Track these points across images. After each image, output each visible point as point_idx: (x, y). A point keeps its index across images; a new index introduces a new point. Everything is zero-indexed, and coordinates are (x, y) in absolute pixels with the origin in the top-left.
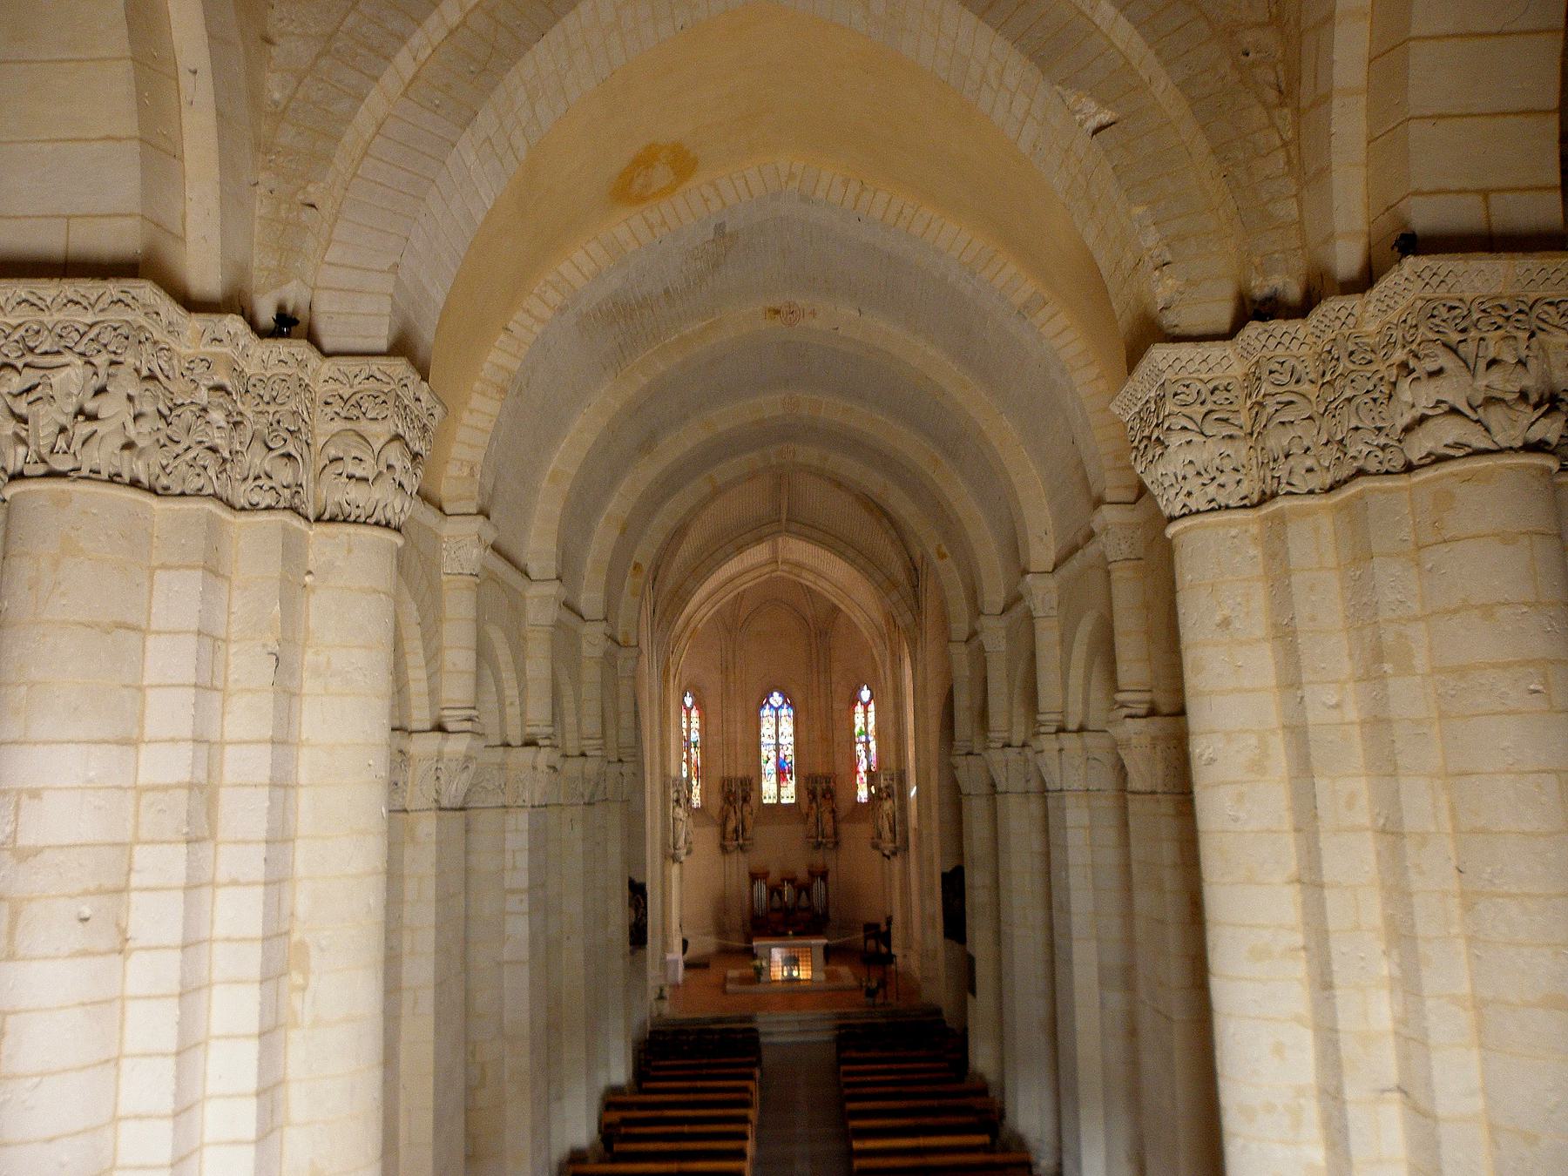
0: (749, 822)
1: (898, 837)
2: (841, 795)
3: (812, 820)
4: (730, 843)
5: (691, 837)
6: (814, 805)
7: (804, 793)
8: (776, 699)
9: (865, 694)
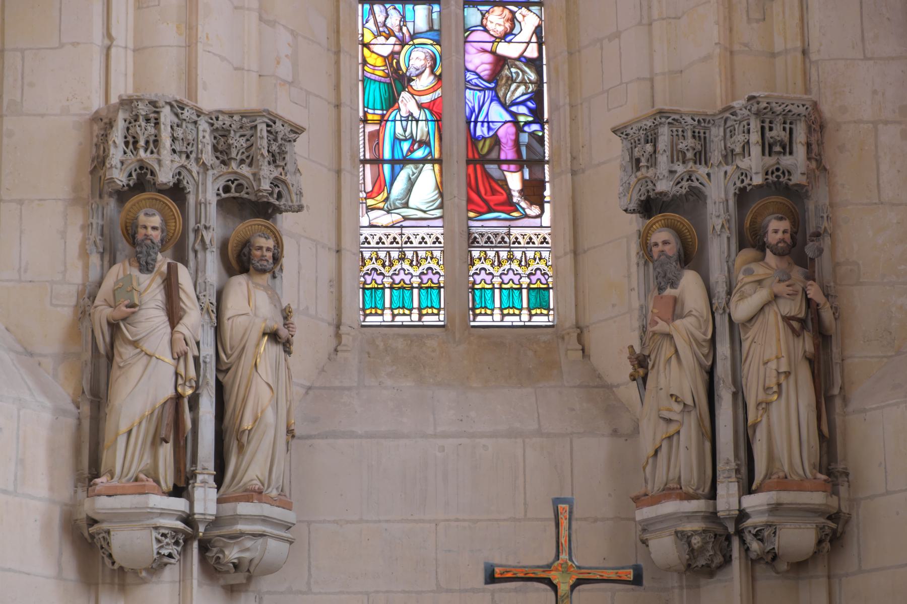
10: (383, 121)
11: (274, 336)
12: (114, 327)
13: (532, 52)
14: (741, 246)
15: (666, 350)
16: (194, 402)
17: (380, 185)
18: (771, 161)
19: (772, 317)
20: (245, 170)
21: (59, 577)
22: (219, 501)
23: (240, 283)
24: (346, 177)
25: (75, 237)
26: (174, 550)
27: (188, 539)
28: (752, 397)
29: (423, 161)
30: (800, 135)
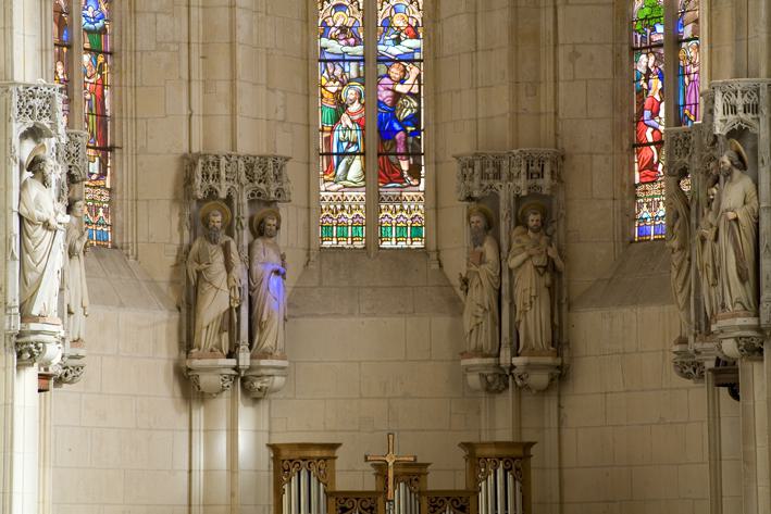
13: (415, 90)
14: (517, 224)
18: (531, 182)
20: (262, 186)
23: (259, 241)
25: (176, 220)
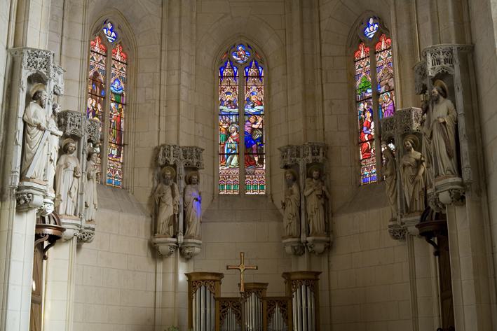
0: (196, 212)
1: (466, 164)
2: (339, 174)
3: (292, 209)
4: (162, 239)
5: (91, 213)
6: (295, 188)
7: (280, 173)
8: (240, 56)
9: (371, 31)
10: (225, 144)
11: (197, 199)
12: (160, 198)
13: (261, 127)
14: (307, 177)
15: (289, 202)
16: (178, 215)
17: (224, 160)
18: (314, 157)
19: (314, 195)
20: (190, 160)
21: (148, 256)
22: (184, 239)
23: (189, 186)
24: (216, 159)
25: (151, 177)
26: (173, 250)
27: (177, 247)
28: (309, 213)
29: (235, 154)
30: (321, 151)
